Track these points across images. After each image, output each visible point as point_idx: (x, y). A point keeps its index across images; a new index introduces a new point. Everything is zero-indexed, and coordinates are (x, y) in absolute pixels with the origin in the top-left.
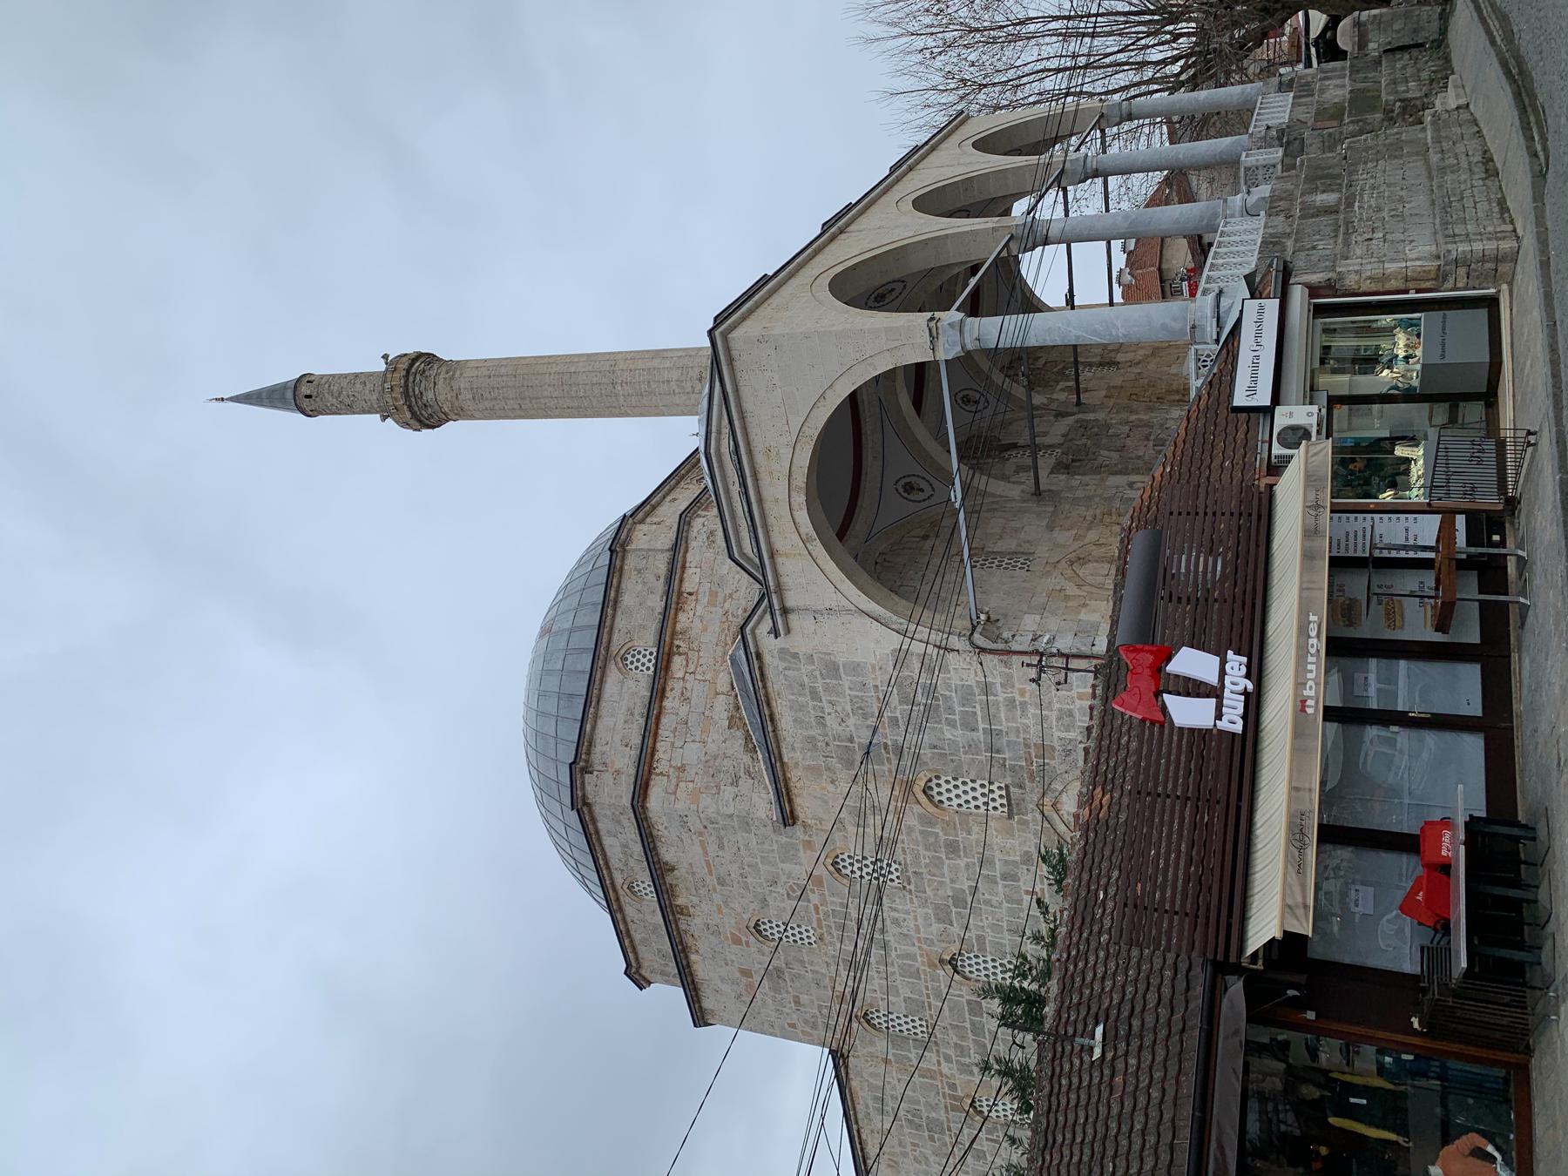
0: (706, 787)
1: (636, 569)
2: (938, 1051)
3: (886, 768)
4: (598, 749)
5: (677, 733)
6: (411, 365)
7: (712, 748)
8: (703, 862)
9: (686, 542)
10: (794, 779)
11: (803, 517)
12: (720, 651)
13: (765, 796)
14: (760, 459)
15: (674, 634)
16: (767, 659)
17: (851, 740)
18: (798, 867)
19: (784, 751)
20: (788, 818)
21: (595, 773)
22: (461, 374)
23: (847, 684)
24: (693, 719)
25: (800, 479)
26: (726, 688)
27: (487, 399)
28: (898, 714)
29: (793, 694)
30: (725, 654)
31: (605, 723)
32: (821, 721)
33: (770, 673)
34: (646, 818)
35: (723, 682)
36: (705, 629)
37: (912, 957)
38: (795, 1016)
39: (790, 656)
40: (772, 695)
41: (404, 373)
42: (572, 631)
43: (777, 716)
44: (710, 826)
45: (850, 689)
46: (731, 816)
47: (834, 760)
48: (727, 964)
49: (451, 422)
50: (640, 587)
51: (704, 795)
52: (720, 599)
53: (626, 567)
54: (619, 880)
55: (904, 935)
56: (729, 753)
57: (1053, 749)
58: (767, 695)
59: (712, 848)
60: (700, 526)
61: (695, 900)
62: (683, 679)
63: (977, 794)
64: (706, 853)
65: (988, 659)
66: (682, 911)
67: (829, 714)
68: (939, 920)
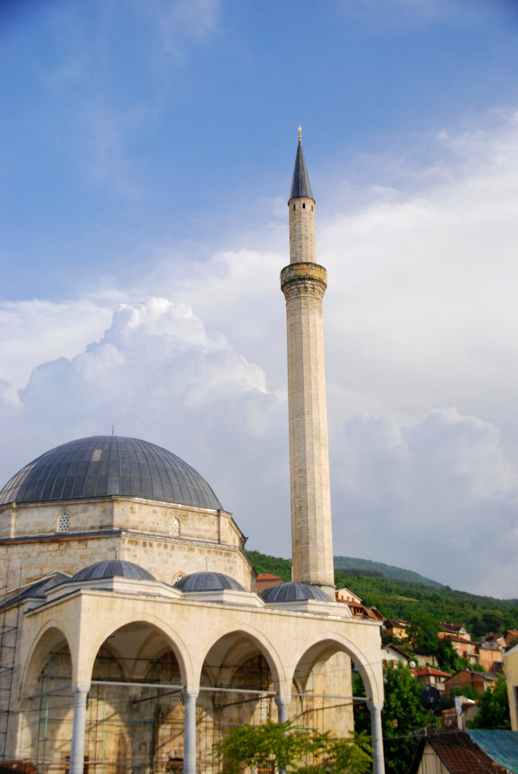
9: (110, 537)
14: (60, 607)
35: (46, 571)
52: (84, 560)
53: (106, 504)
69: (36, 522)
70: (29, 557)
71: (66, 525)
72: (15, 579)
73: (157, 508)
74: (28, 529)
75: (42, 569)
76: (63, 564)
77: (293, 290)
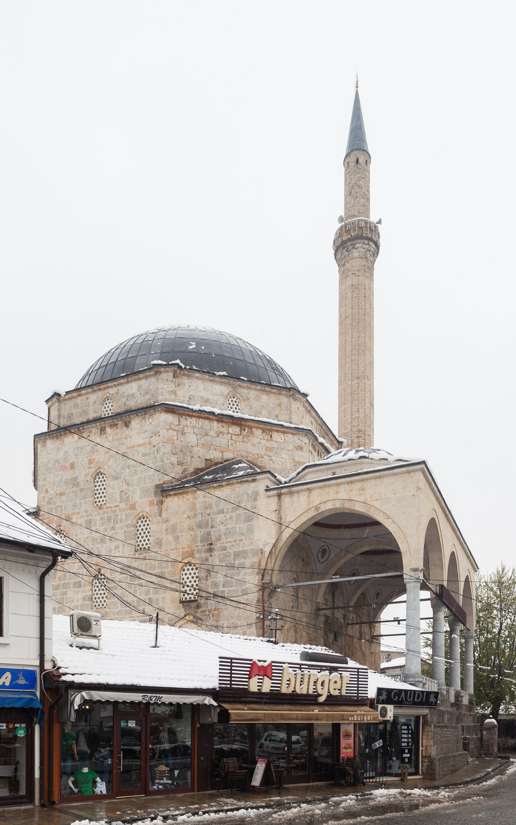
0: (175, 447)
1: (281, 403)
3: (199, 544)
5: (201, 430)
7: (195, 449)
8: (133, 444)
9: (297, 434)
10: (187, 497)
12: (244, 454)
15: (251, 428)
16: (253, 485)
17: (212, 527)
18: (139, 497)
23: (241, 526)
24: (209, 439)
29: (234, 497)
30: (242, 456)
33: (245, 486)
38: (52, 493)
39: (255, 497)
40: (233, 487)
43: (222, 489)
44: (155, 449)
45: (240, 527)
46: (162, 461)
47: (200, 518)
48: (75, 455)
49: (338, 269)
50: (271, 406)
51: (171, 446)
53: (281, 397)
55: (111, 551)
56: (194, 459)
58: (233, 484)
59: (142, 450)
60: (305, 442)
61: (111, 438)
64: (139, 446)
66: (103, 430)
67: (225, 516)
70: (206, 435)
72: (192, 457)
76: (247, 452)
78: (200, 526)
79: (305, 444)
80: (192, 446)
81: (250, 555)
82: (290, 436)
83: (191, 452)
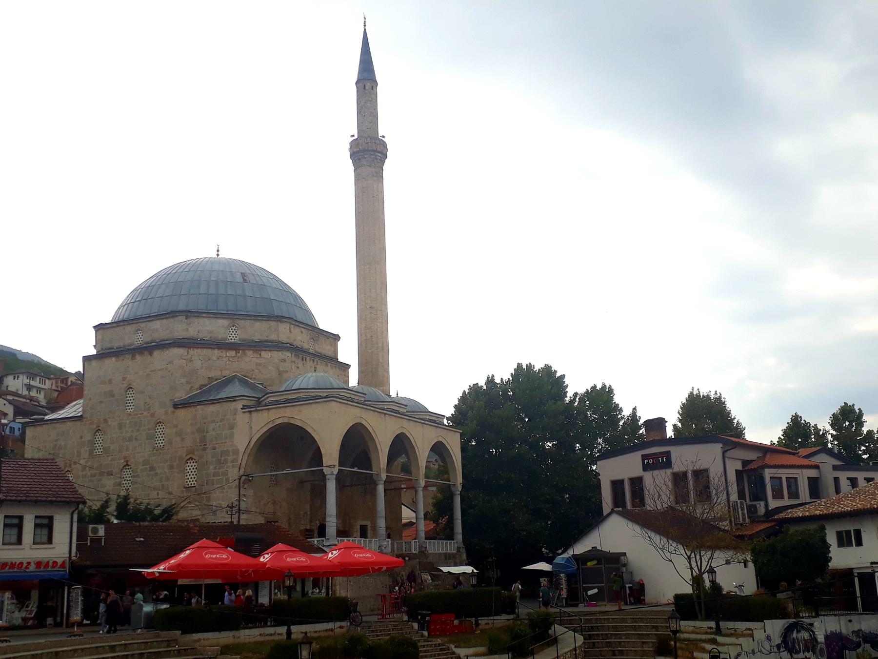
2: (89, 458)
3: (198, 445)
4: (196, 320)
6: (379, 152)
11: (280, 421)
13: (184, 395)
14: (297, 408)
16: (234, 403)
17: (207, 432)
19: (201, 406)
20: (176, 406)
21: (186, 321)
22: (374, 181)
25: (292, 421)
26: (224, 374)
27: (363, 195)
28: (217, 450)
31: (207, 322)
32: (213, 421)
33: (229, 404)
34: (171, 347)
35: (227, 373)
36: (246, 363)
37: (127, 450)
41: (375, 149)
42: (245, 297)
43: (213, 405)
46: (174, 382)
53: (271, 322)
54: (142, 325)
57: (209, 502)
60: (287, 355)
62: (226, 356)
63: (191, 476)
64: (159, 370)
65: (237, 481)
66: (133, 358)
68: (143, 461)
69: (208, 330)
71: (235, 336)
72: (197, 377)
73: (303, 330)
74: (201, 336)
75: (221, 371)
77: (365, 158)
78: (199, 431)
79: (288, 357)
80: (198, 369)
81: (231, 453)
82: (275, 352)
83: (197, 373)
